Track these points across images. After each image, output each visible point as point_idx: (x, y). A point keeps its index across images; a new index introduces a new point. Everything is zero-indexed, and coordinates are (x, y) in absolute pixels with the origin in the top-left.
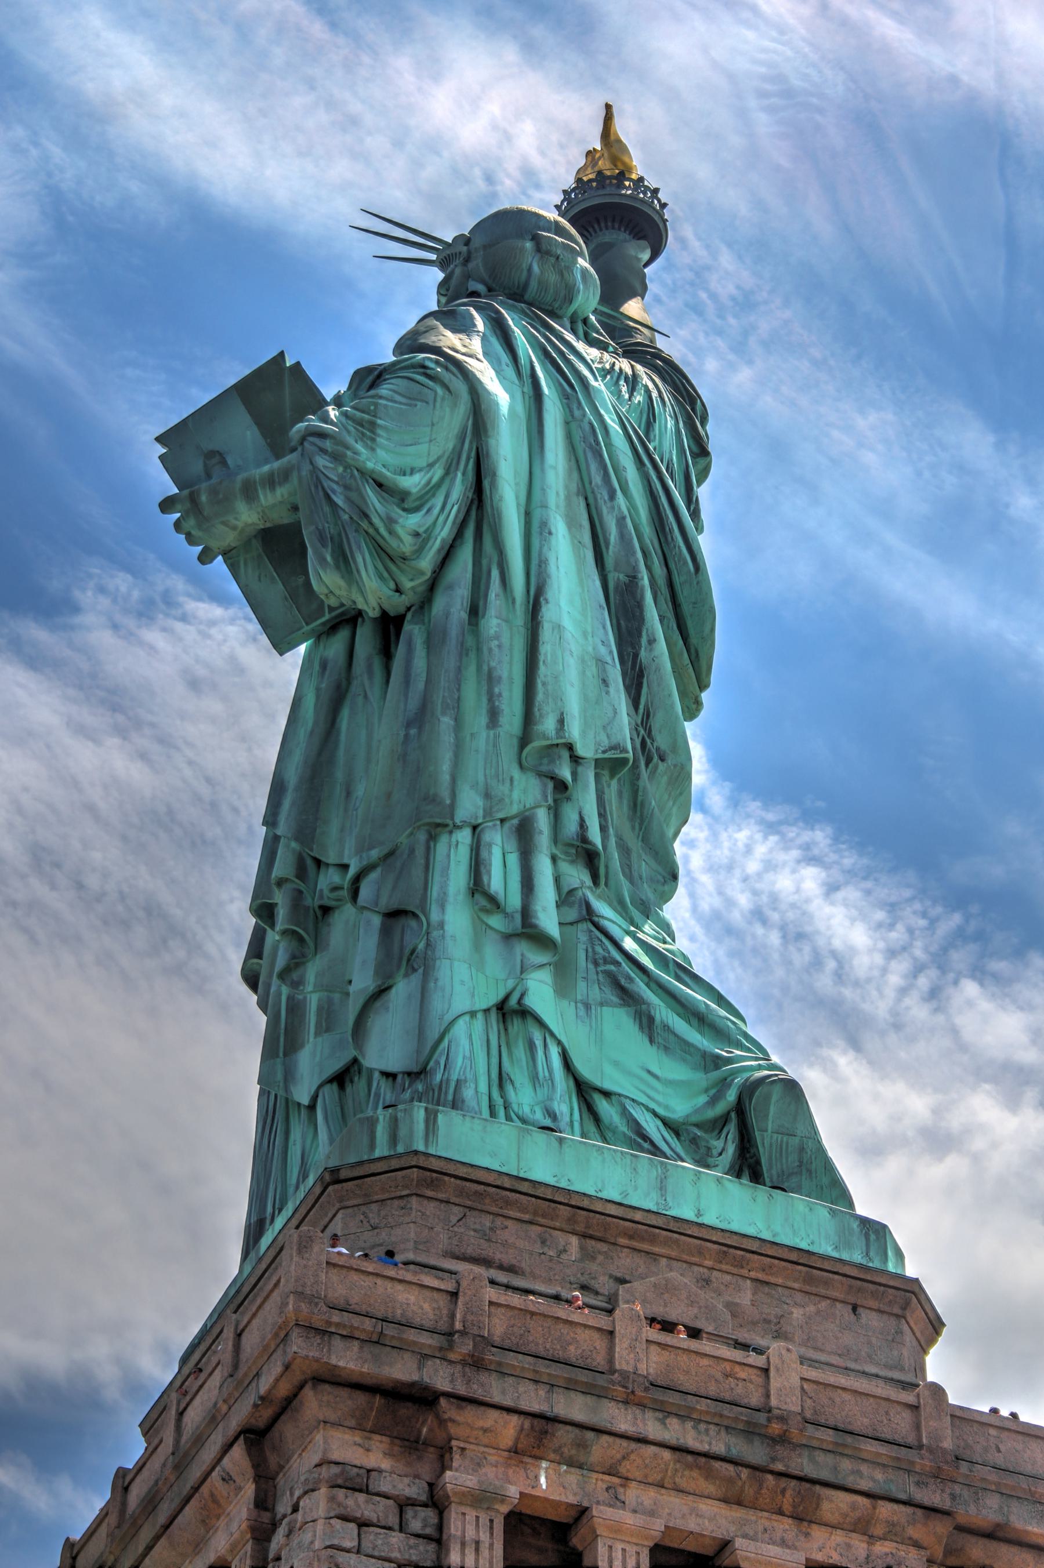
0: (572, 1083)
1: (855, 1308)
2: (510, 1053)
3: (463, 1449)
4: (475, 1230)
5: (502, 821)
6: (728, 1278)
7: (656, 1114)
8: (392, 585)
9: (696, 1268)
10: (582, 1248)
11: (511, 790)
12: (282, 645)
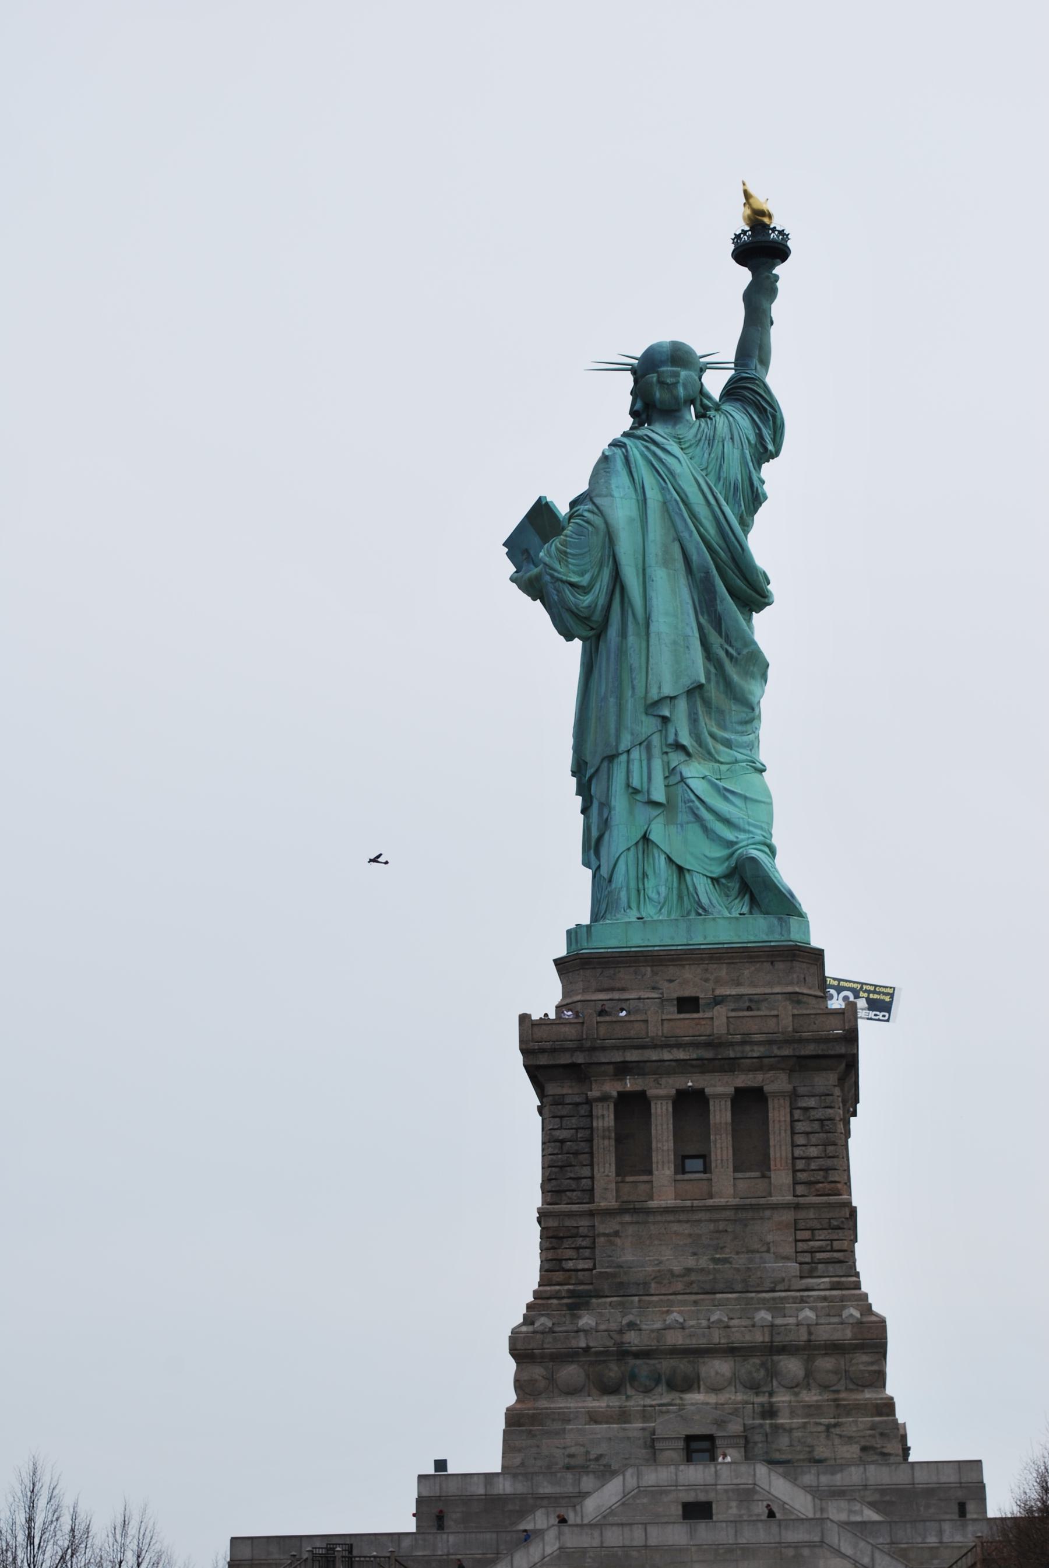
0: (674, 867)
1: (772, 963)
2: (648, 861)
3: (596, 1080)
4: (607, 977)
5: (640, 744)
6: (715, 966)
7: (707, 877)
8: (589, 628)
9: (701, 966)
10: (652, 971)
11: (642, 728)
12: (569, 638)
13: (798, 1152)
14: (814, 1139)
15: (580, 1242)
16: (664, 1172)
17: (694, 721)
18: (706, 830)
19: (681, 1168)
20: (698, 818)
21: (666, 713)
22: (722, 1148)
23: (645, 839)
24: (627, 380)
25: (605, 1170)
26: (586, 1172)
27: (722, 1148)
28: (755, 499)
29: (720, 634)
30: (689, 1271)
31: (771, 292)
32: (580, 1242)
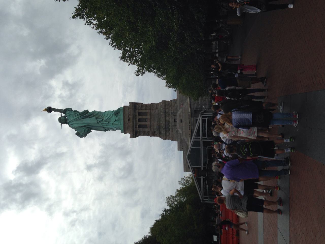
13: (145, 109)
14: (143, 107)
15: (154, 132)
16: (147, 123)
17: (99, 119)
18: (111, 117)
19: (146, 121)
20: (110, 118)
21: (98, 122)
22: (144, 117)
23: (112, 124)
24: (63, 124)
25: (146, 129)
26: (147, 132)
27: (144, 117)
28: (76, 111)
29: (90, 115)
30: (157, 121)
31: (54, 109)
32: (154, 132)
